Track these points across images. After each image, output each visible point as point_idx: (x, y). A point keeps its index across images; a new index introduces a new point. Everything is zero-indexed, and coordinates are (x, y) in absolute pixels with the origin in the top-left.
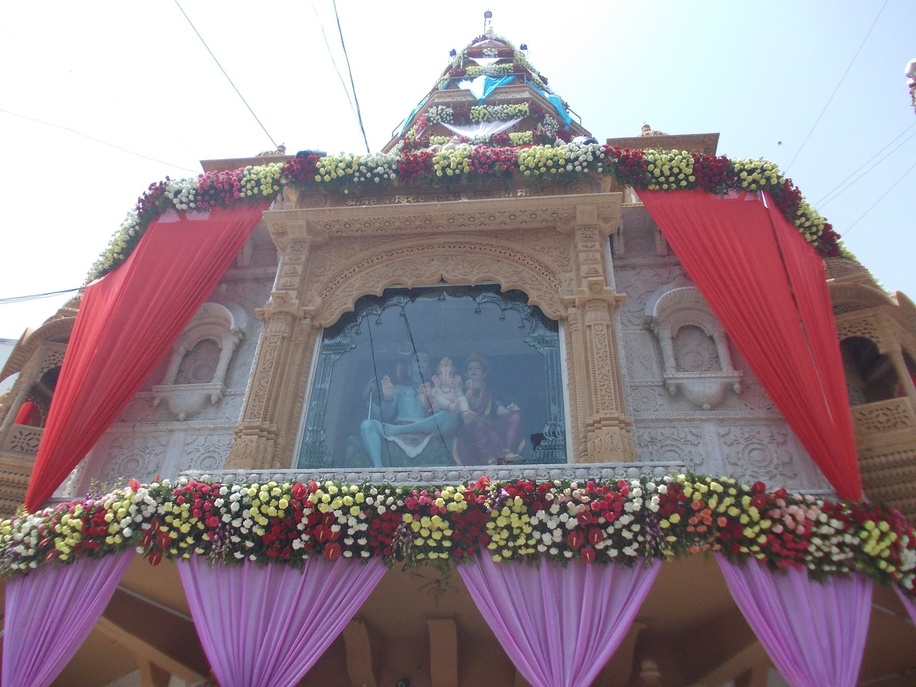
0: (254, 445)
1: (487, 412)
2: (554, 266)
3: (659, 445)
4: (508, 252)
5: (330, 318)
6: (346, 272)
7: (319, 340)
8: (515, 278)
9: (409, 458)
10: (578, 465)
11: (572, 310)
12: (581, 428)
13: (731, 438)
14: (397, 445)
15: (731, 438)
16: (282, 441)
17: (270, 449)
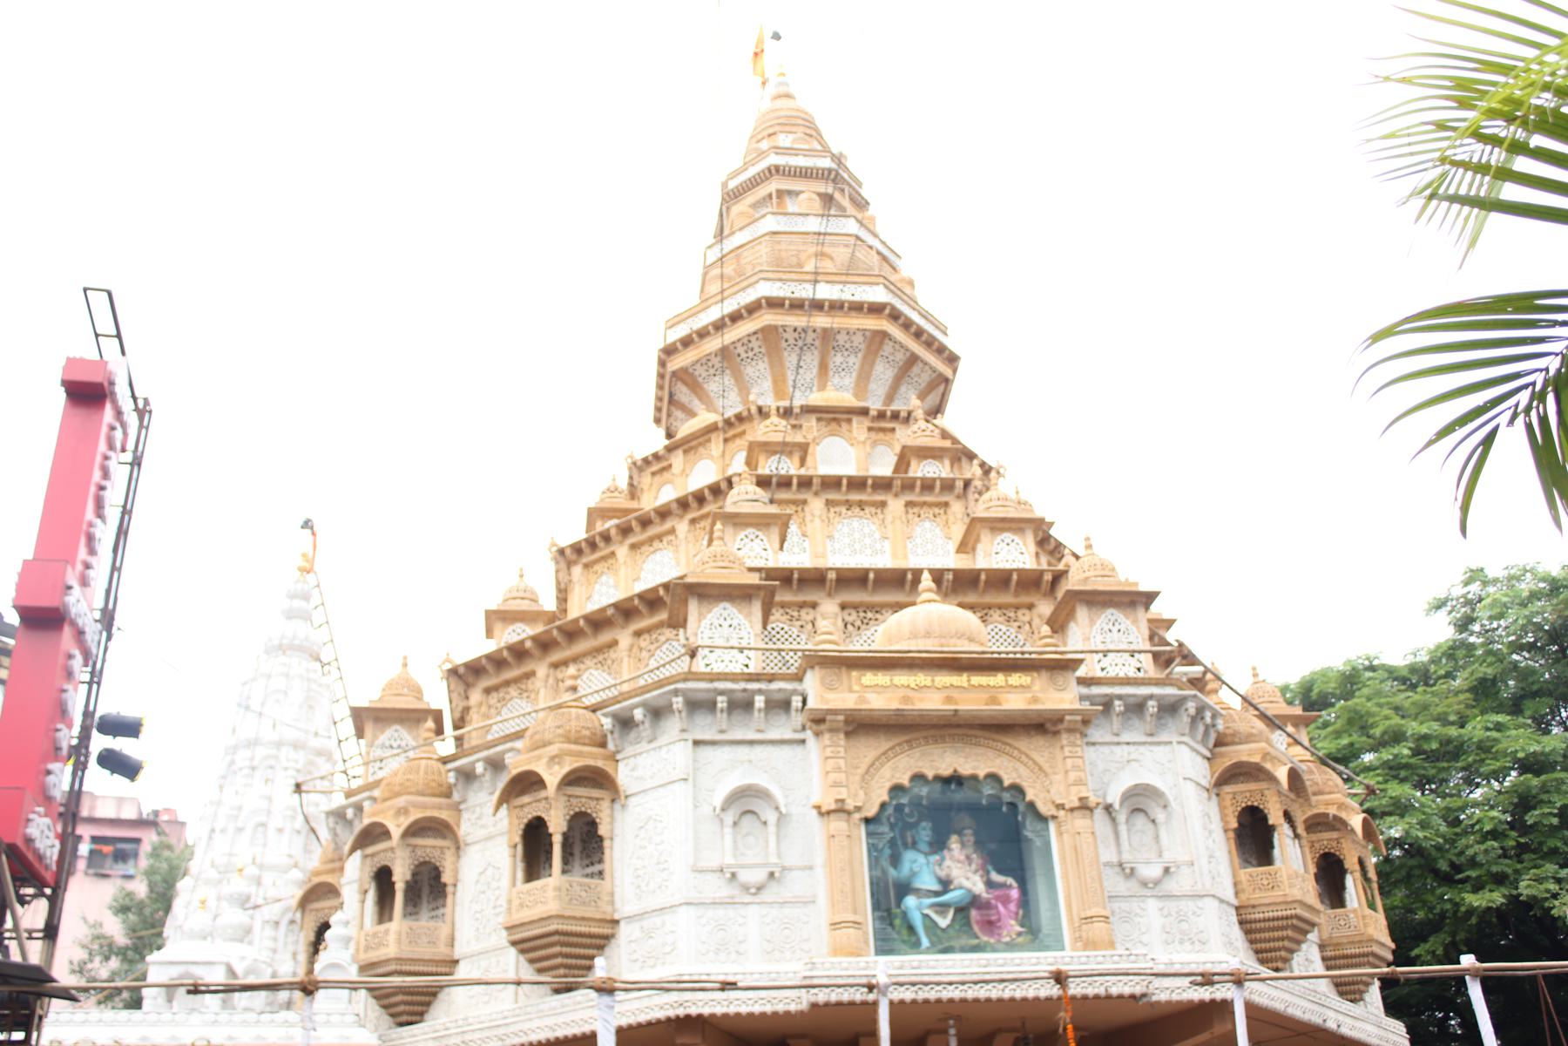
2: (1046, 766)
5: (871, 811)
11: (1062, 813)
12: (1076, 918)
13: (1165, 911)
15: (1165, 911)
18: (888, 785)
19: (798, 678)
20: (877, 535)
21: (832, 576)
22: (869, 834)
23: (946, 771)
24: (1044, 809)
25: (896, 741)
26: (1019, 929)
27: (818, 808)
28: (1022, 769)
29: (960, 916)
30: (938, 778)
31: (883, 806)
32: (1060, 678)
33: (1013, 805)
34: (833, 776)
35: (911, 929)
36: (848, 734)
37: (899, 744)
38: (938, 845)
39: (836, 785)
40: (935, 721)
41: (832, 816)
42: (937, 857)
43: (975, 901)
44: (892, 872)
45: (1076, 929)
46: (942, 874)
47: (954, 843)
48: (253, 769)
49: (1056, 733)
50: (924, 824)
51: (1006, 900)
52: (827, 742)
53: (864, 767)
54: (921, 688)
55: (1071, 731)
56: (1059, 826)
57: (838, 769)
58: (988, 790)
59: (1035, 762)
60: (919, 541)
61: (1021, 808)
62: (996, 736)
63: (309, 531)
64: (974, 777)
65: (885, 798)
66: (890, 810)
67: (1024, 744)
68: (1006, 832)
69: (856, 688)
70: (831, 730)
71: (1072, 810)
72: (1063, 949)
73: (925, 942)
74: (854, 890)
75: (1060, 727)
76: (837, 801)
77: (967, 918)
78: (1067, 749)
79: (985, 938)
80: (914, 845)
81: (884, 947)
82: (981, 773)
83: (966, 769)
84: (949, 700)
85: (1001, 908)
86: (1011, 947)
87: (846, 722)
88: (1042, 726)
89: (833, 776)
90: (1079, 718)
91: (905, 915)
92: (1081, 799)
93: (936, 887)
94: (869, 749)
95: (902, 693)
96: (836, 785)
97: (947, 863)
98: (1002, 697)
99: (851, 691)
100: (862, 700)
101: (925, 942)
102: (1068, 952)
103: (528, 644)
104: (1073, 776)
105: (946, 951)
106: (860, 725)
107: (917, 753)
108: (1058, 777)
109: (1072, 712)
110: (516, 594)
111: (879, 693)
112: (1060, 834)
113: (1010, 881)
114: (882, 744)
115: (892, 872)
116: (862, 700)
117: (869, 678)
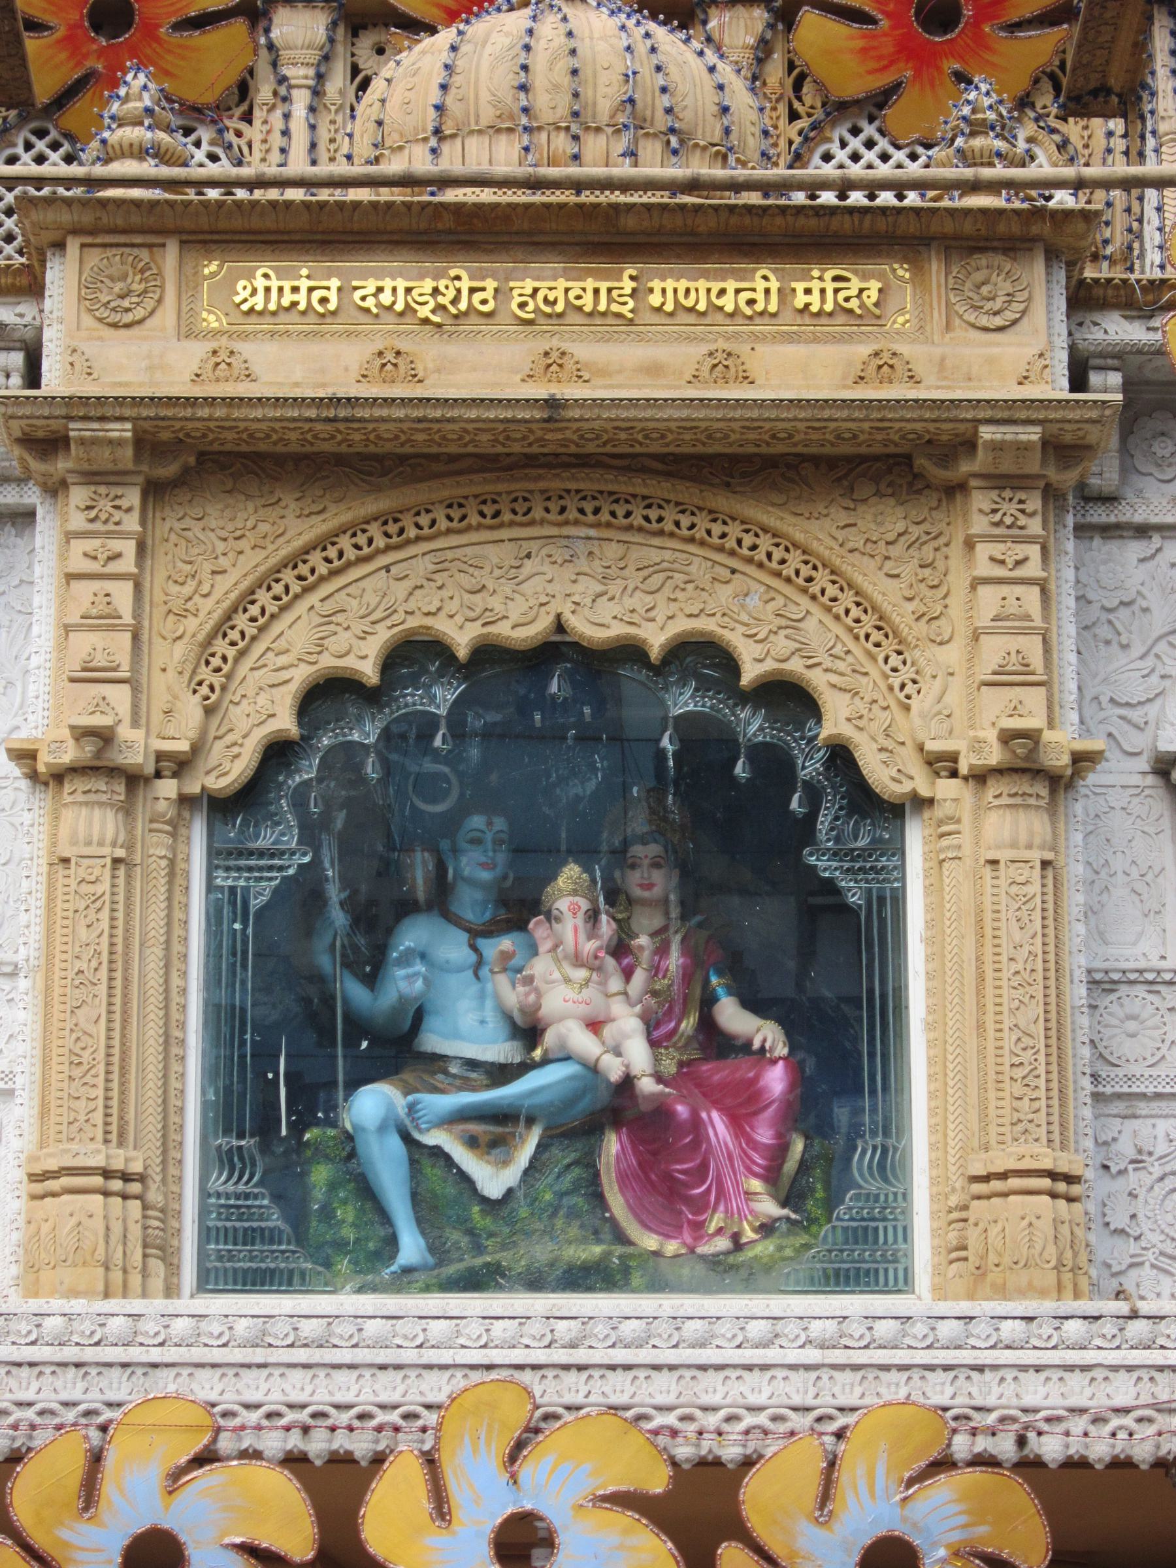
0: (98, 1224)
1: (688, 1025)
2: (902, 615)
3: (1157, 1171)
4: (765, 543)
5: (229, 768)
6: (263, 597)
8: (782, 644)
9: (485, 1200)
10: (943, 1308)
11: (947, 788)
14: (448, 1158)
16: (155, 1196)
17: (136, 1231)
18: (301, 676)
19: (31, 286)
22: (216, 855)
23: (521, 626)
24: (879, 773)
25: (338, 516)
26: (769, 1208)
27: (25, 756)
28: (819, 630)
29: (563, 1155)
30: (488, 654)
31: (278, 754)
32: (999, 278)
33: (775, 765)
34: (85, 644)
35: (367, 1192)
36: (156, 492)
37: (352, 529)
39: (90, 675)
40: (485, 444)
41: (74, 787)
43: (616, 1105)
44: (355, 991)
45: (958, 1216)
47: (568, 891)
49: (955, 490)
50: (477, 821)
51: (742, 1105)
52: (78, 521)
53: (210, 610)
55: (1000, 482)
57: (105, 620)
58: (684, 701)
59: (863, 601)
61: (810, 768)
62: (722, 502)
64: (630, 652)
65: (286, 723)
66: (308, 770)
67: (822, 529)
68: (764, 862)
70: (92, 477)
71: (980, 777)
72: (904, 1284)
73: (411, 1247)
74: (119, 1062)
75: (965, 467)
76: (82, 734)
77: (589, 1163)
78: (983, 550)
79: (650, 1242)
80: (440, 900)
81: (246, 1257)
82: (656, 639)
83: (597, 625)
84: (553, 363)
85: (718, 1127)
86: (729, 1271)
87: (147, 444)
88: (895, 462)
89: (85, 644)
90: (1032, 434)
91: (348, 1147)
92: (1007, 737)
93: (500, 1050)
94: (226, 547)
95: (380, 337)
96: (90, 675)
97: (541, 966)
100: (220, 361)
101: (411, 1247)
102: (920, 1300)
104: (994, 650)
105: (472, 1282)
106: (194, 459)
107: (418, 562)
108: (952, 655)
109: (1008, 412)
111: (290, 338)
113: (767, 1034)
114: (295, 525)
115: (355, 991)
117: (262, 283)
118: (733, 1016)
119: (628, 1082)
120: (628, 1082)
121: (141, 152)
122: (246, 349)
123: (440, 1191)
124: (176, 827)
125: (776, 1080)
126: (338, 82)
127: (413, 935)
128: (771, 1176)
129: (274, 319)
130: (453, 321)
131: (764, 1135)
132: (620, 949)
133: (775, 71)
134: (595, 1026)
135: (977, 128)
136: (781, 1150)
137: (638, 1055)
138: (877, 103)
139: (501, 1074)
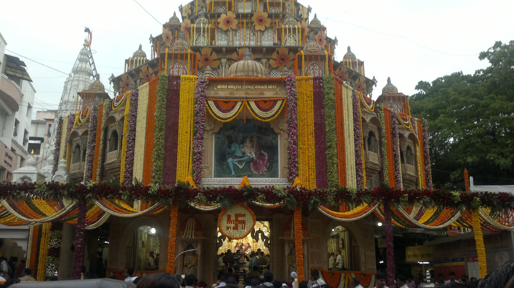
7: (214, 136)
11: (282, 132)
20: (252, 34)
21: (224, 49)
35: (229, 168)
38: (243, 142)
42: (242, 145)
46: (243, 150)
48: (67, 110)
51: (263, 160)
54: (237, 90)
56: (281, 136)
60: (266, 36)
63: (87, 33)
69: (215, 89)
73: (233, 173)
79: (255, 172)
85: (261, 162)
86: (262, 176)
91: (228, 163)
93: (241, 155)
97: (245, 148)
98: (265, 92)
99: (214, 90)
101: (233, 173)
103: (133, 72)
110: (137, 54)
112: (281, 139)
113: (266, 154)
115: (228, 150)
116: (216, 93)
118: (262, 152)
119: (253, 158)
120: (253, 158)
121: (209, 74)
122: (218, 92)
123: (236, 167)
124: (212, 135)
125: (267, 158)
126: (227, 66)
127: (233, 145)
128: (266, 167)
129: (222, 89)
130: (237, 90)
131: (265, 162)
132: (252, 146)
133: (267, 65)
134: (250, 153)
135: (285, 72)
136: (267, 165)
137: (254, 156)
138: (277, 68)
139: (242, 157)
